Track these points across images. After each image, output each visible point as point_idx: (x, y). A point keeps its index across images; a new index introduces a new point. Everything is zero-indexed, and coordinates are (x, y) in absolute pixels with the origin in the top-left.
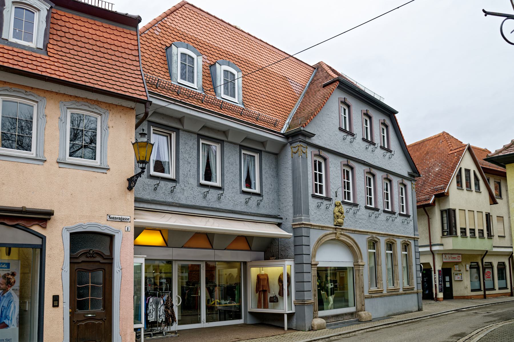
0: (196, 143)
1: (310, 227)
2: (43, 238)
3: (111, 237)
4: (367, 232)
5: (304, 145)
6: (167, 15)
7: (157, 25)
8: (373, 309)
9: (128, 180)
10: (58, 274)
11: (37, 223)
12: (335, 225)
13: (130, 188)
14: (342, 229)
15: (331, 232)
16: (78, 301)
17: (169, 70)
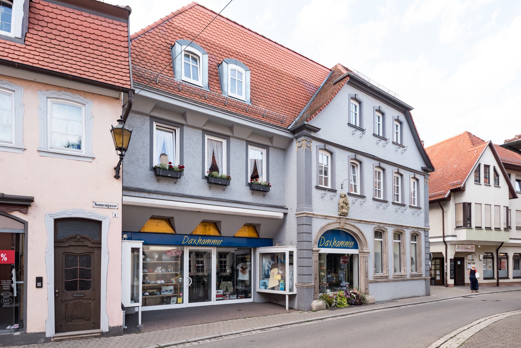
0: (201, 138)
1: (312, 216)
2: (25, 223)
3: (98, 224)
4: (374, 222)
5: (309, 139)
6: (175, 15)
7: (163, 25)
8: (376, 293)
9: (115, 169)
10: (40, 258)
11: (17, 209)
12: (340, 215)
13: (117, 177)
14: (347, 219)
15: (335, 221)
16: (66, 282)
17: (172, 69)
